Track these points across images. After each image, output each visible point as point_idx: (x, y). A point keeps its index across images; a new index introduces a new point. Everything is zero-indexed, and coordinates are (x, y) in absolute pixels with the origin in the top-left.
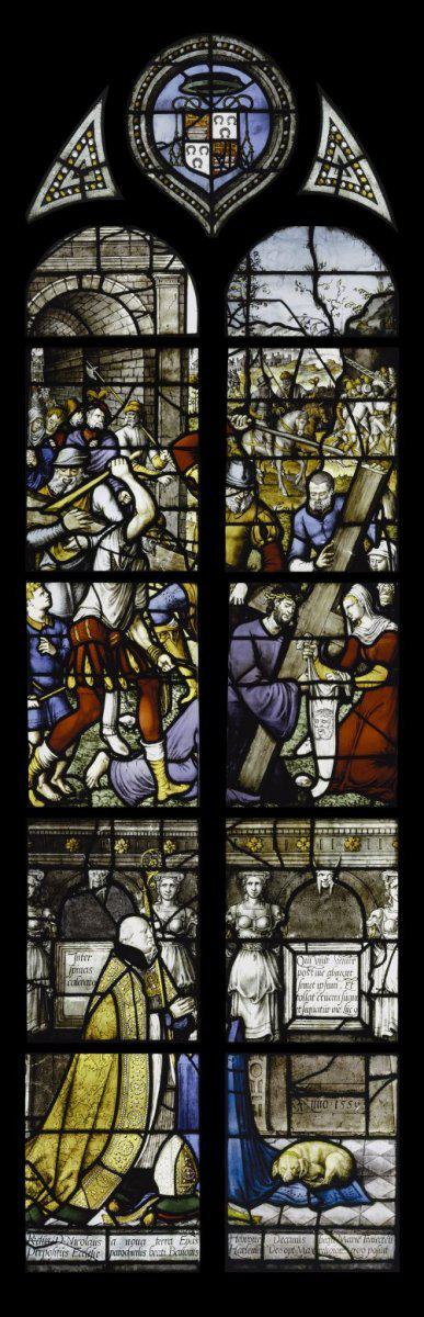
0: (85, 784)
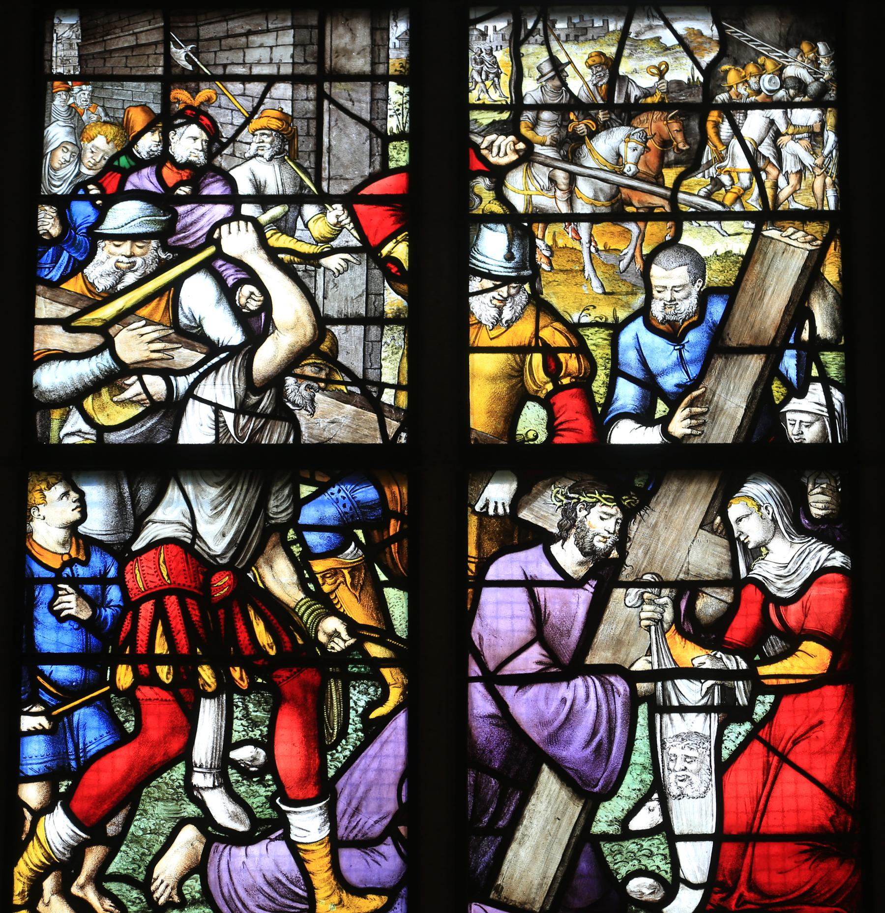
0: (149, 894)
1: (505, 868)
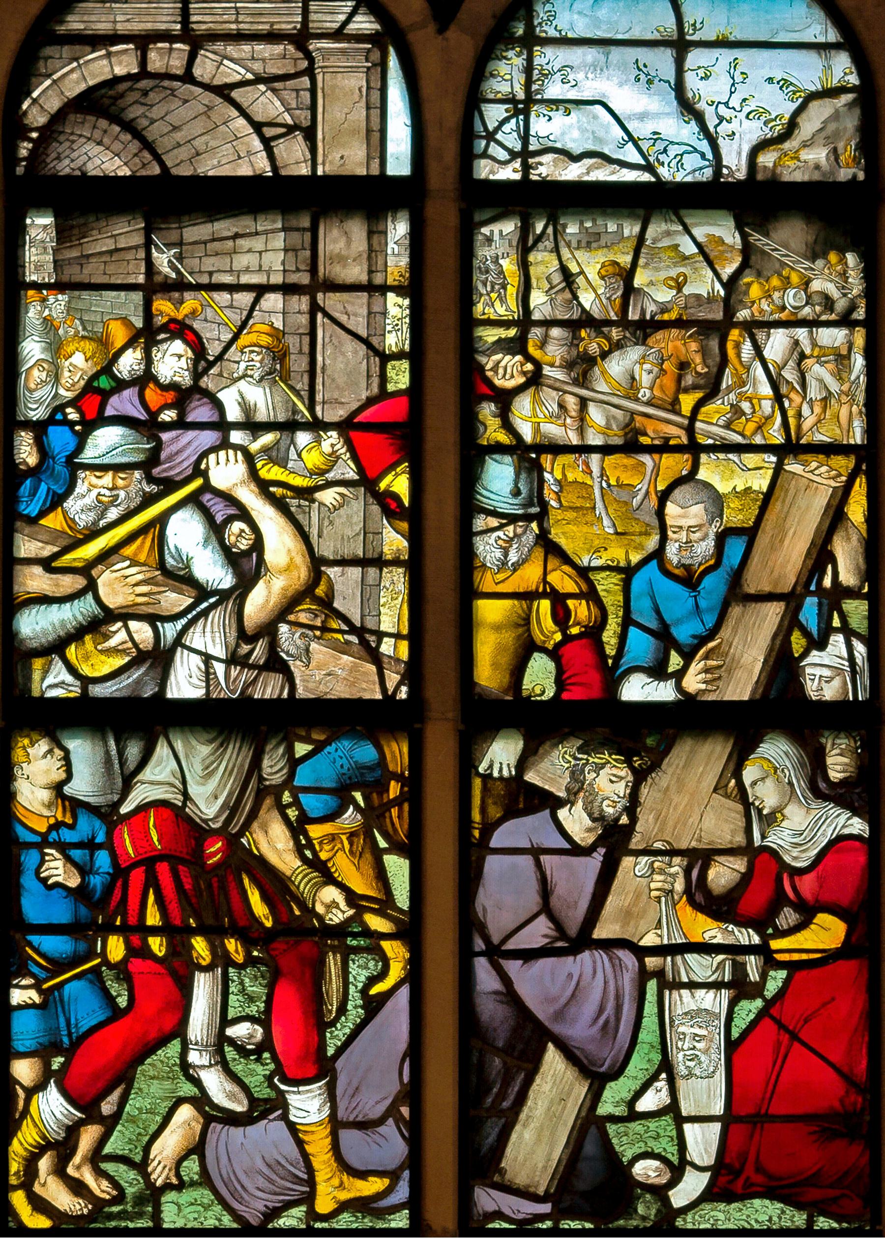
0: (146, 1176)
1: (509, 1150)
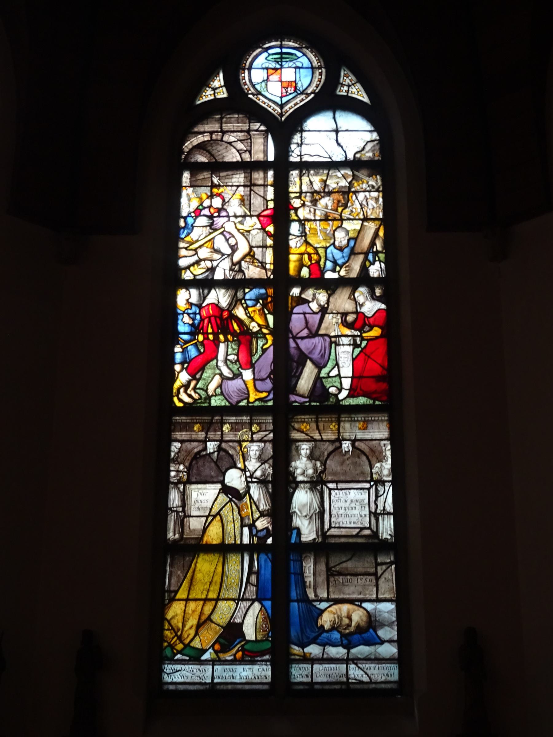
0: (207, 393)
1: (298, 386)
